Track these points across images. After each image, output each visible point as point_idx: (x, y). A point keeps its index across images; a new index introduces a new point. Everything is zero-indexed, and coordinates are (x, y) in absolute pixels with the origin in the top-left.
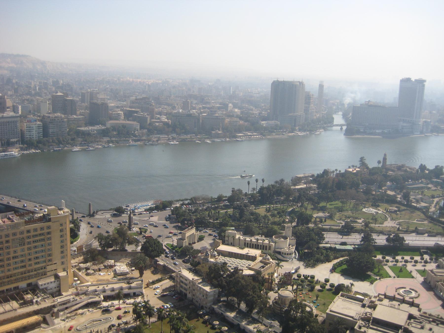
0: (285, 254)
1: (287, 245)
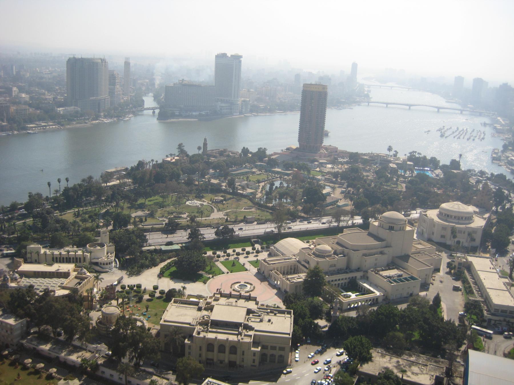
0: (104, 264)
1: (105, 253)
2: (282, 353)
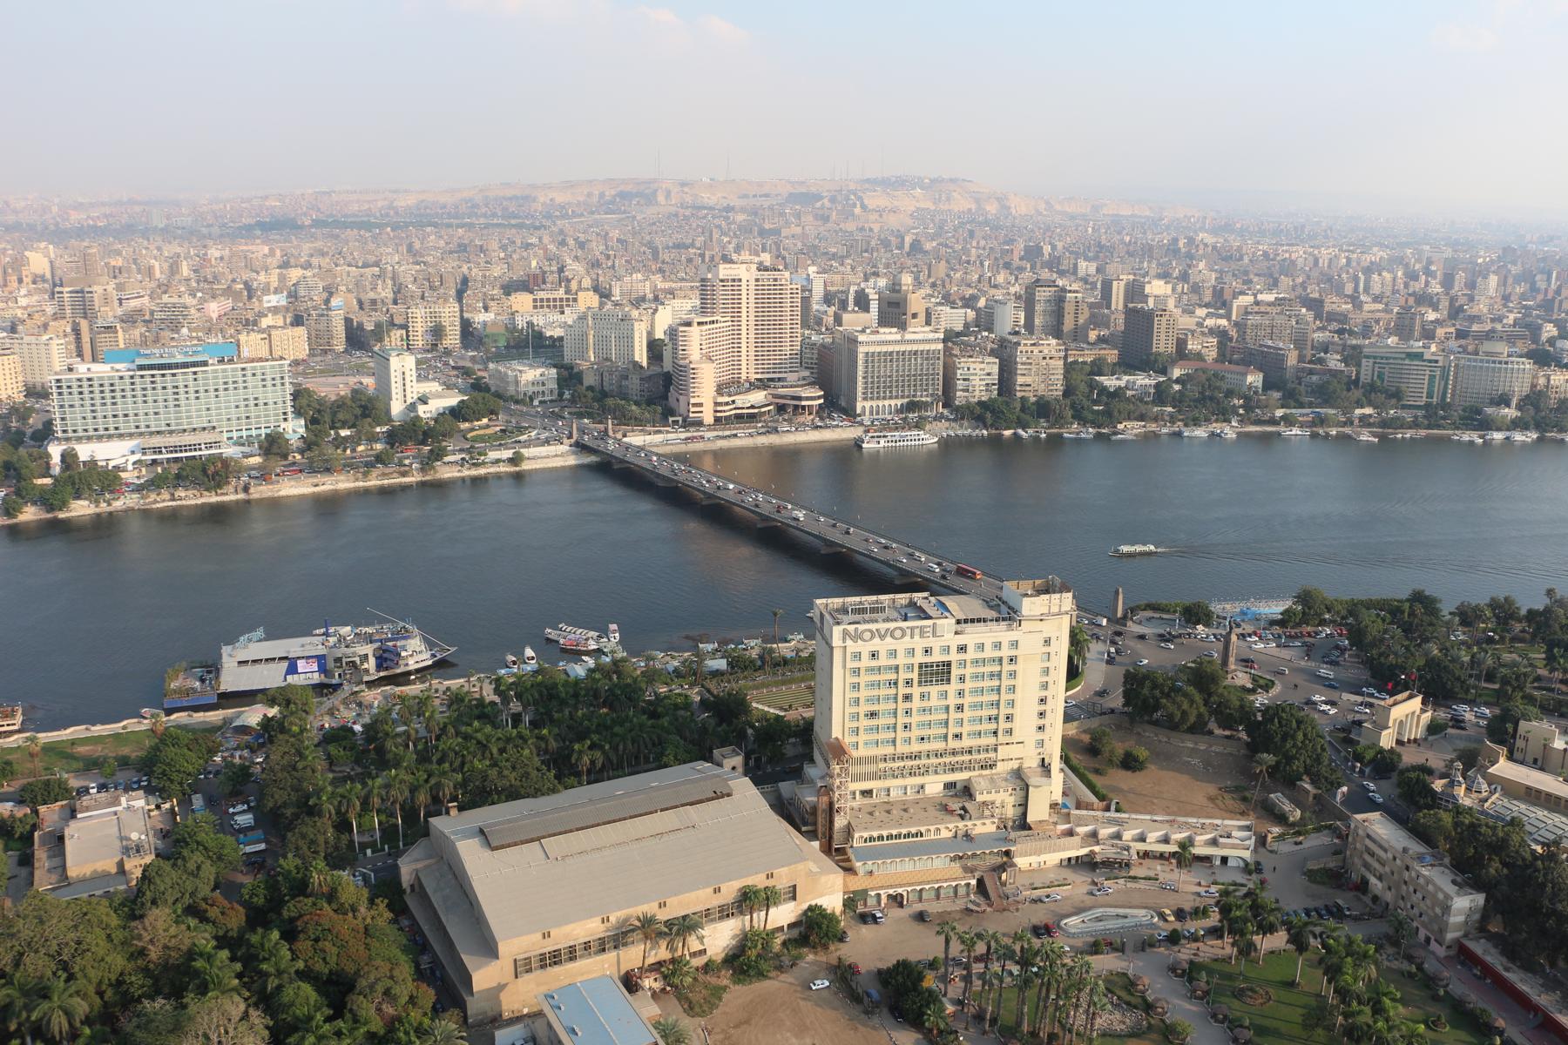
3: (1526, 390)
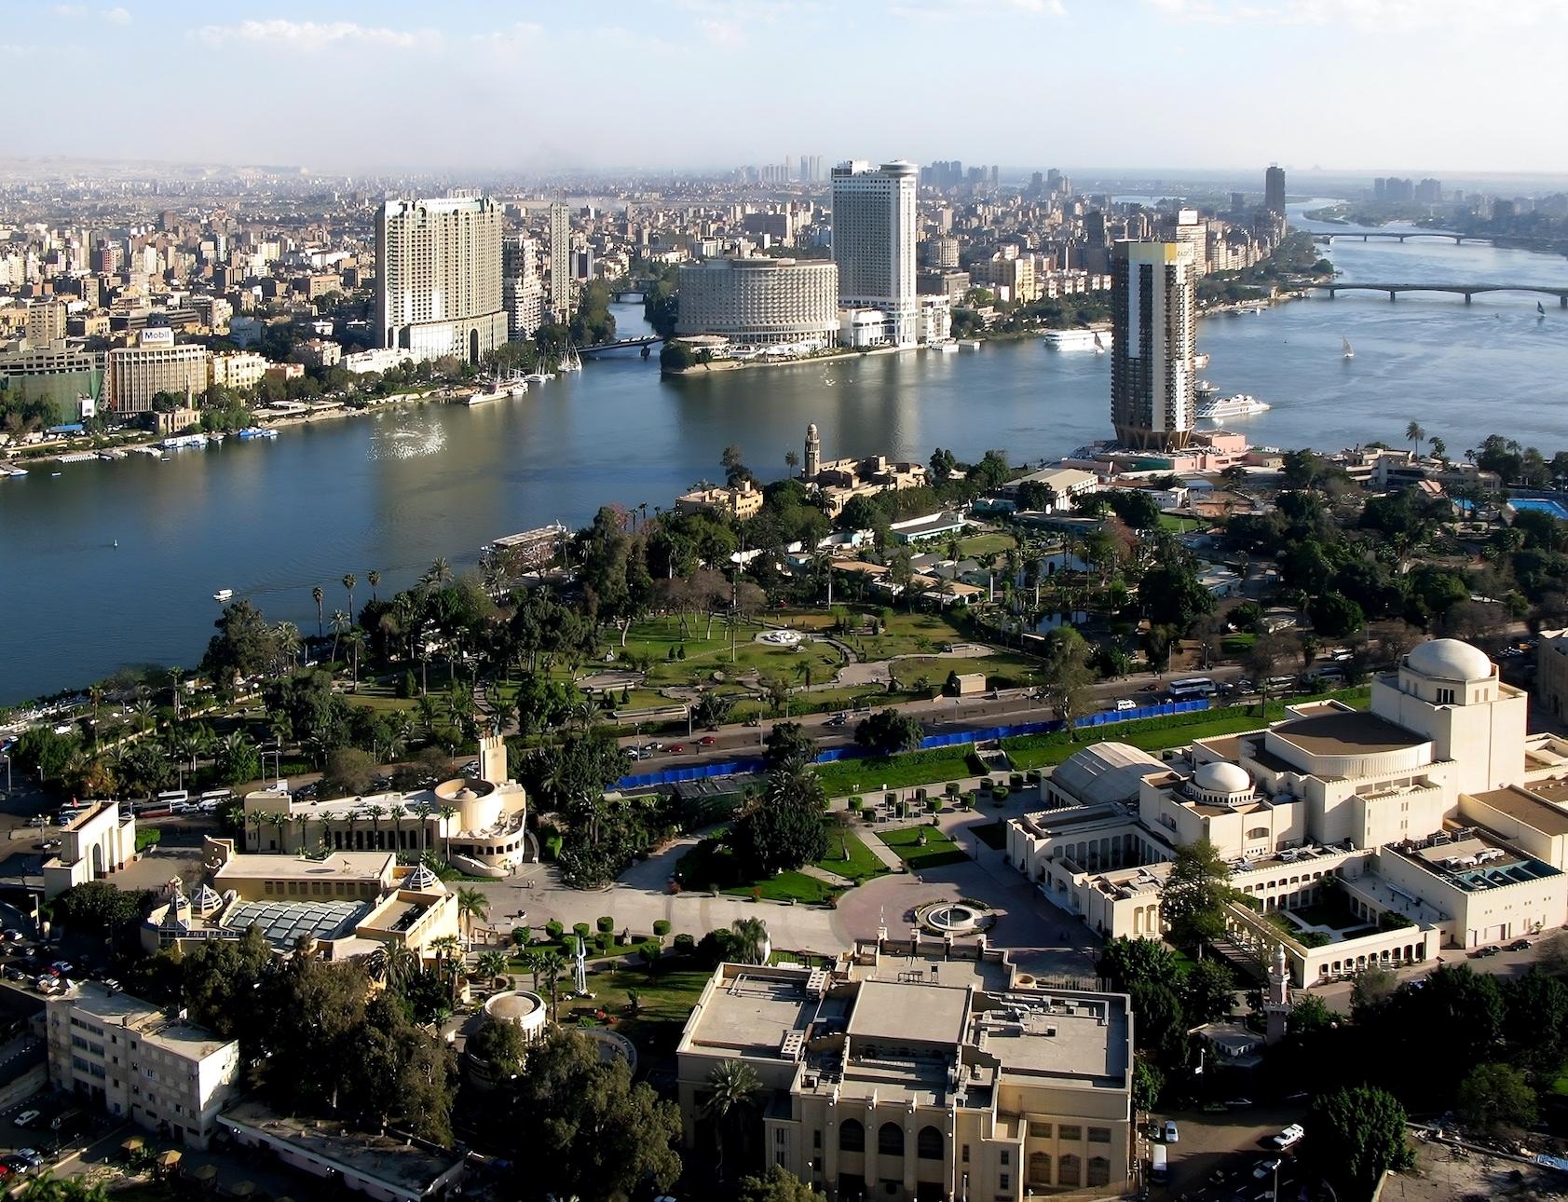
2: (1099, 1149)
3: (203, 387)
